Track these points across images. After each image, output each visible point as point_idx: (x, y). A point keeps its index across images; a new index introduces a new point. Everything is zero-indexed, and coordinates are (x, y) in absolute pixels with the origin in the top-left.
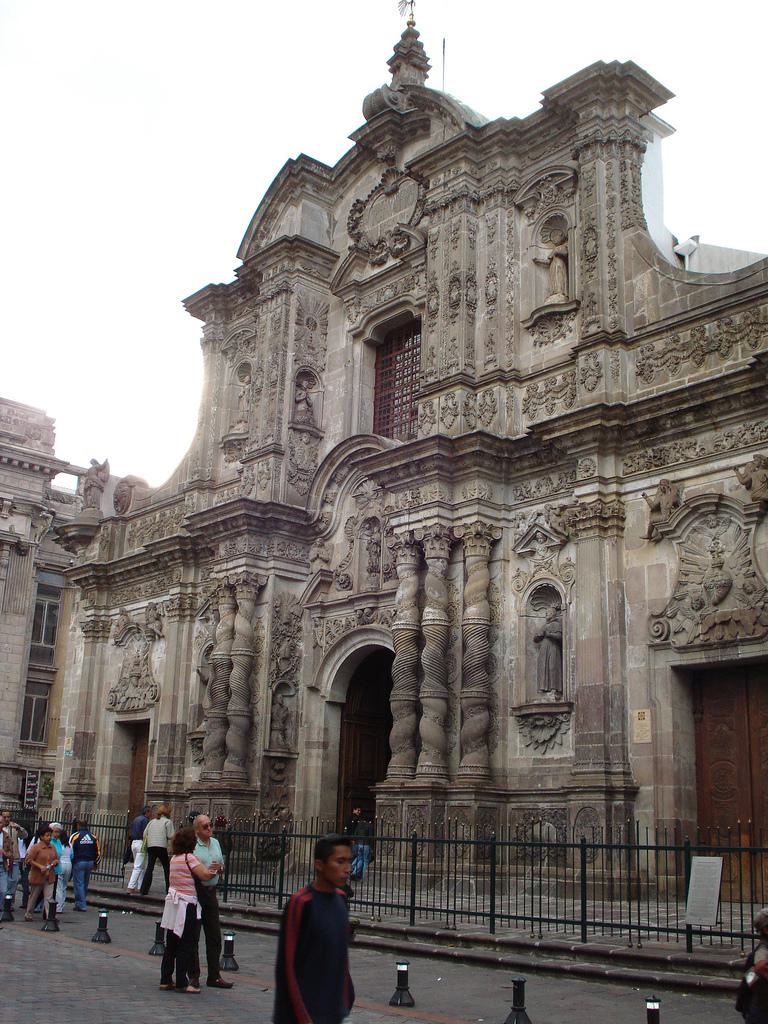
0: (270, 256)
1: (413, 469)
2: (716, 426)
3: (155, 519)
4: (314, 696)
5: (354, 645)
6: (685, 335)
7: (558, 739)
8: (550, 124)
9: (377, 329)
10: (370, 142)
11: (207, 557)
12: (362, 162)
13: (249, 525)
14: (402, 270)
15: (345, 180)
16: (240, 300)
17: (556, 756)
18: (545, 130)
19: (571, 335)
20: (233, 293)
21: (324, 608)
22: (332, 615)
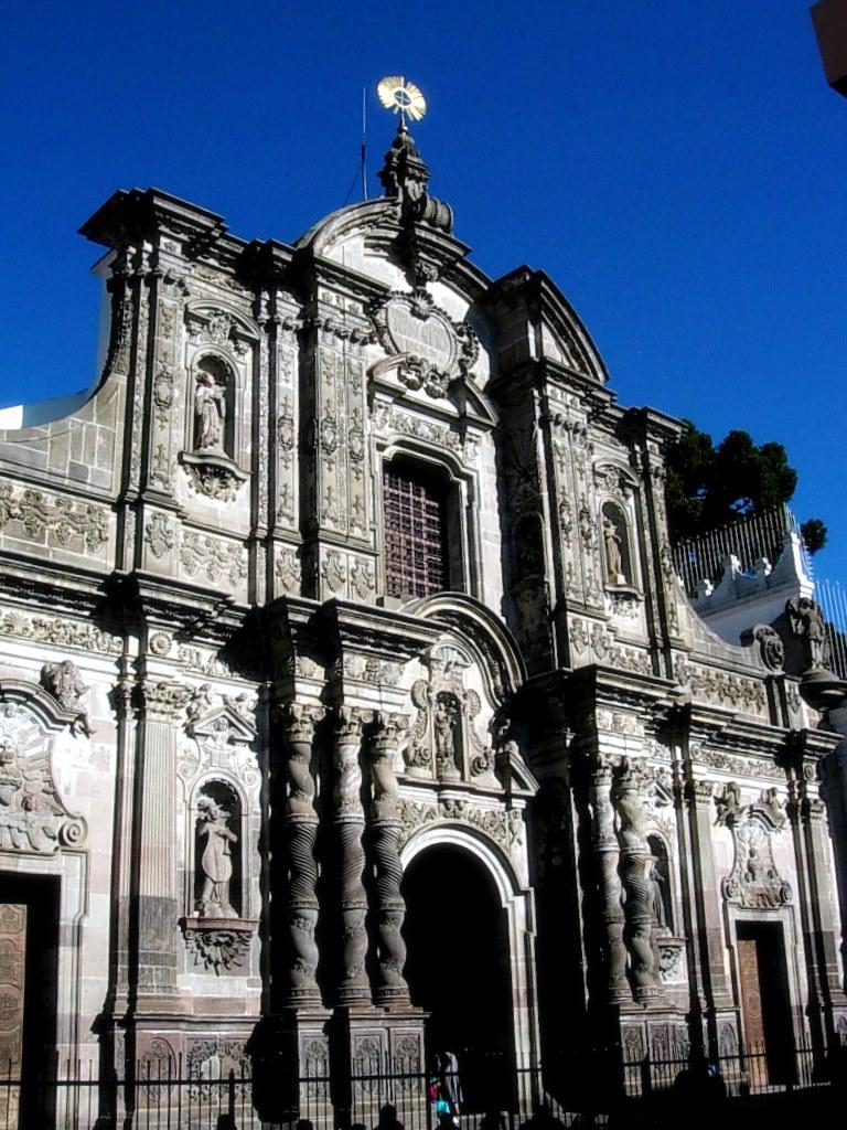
2: (746, 754)
3: (10, 489)
6: (713, 671)
7: (675, 968)
9: (397, 455)
11: (208, 636)
17: (674, 983)
19: (636, 619)
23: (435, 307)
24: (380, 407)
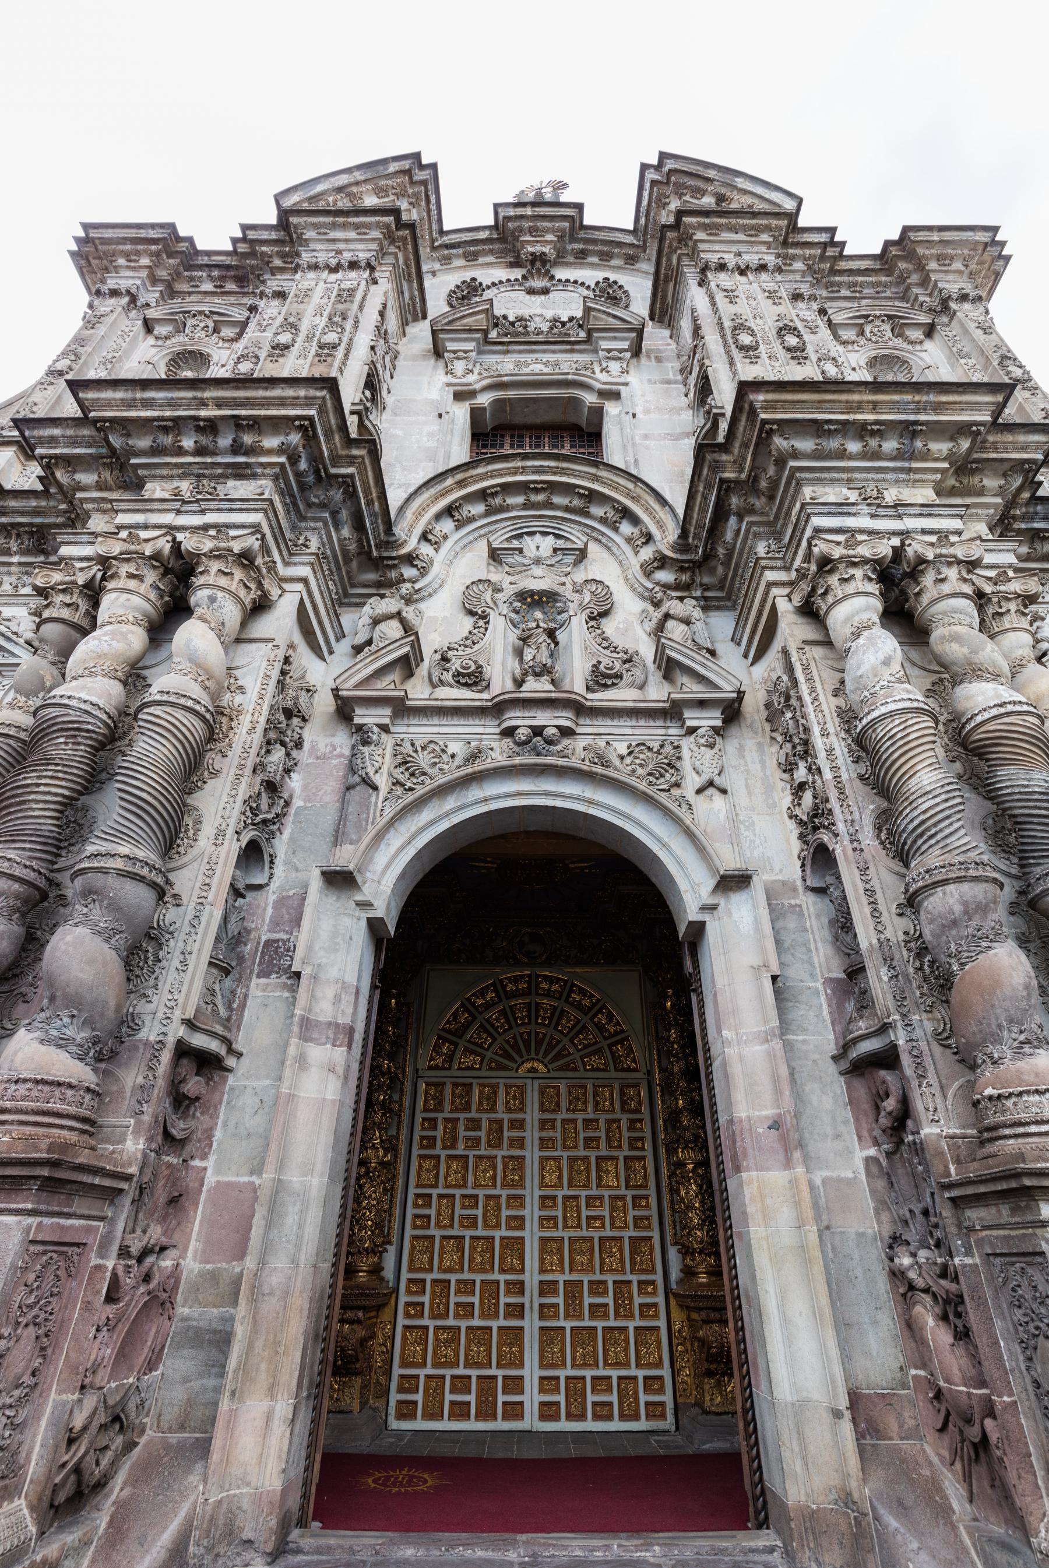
0: (344, 226)
1: (890, 445)
4: (332, 901)
5: (486, 800)
8: (873, 279)
9: (498, 403)
10: (521, 230)
12: (485, 253)
13: (294, 459)
14: (572, 351)
15: (447, 259)
16: (208, 287)
18: (863, 285)
20: (200, 267)
21: (401, 708)
22: (419, 730)
23: (560, 280)
24: (458, 359)
